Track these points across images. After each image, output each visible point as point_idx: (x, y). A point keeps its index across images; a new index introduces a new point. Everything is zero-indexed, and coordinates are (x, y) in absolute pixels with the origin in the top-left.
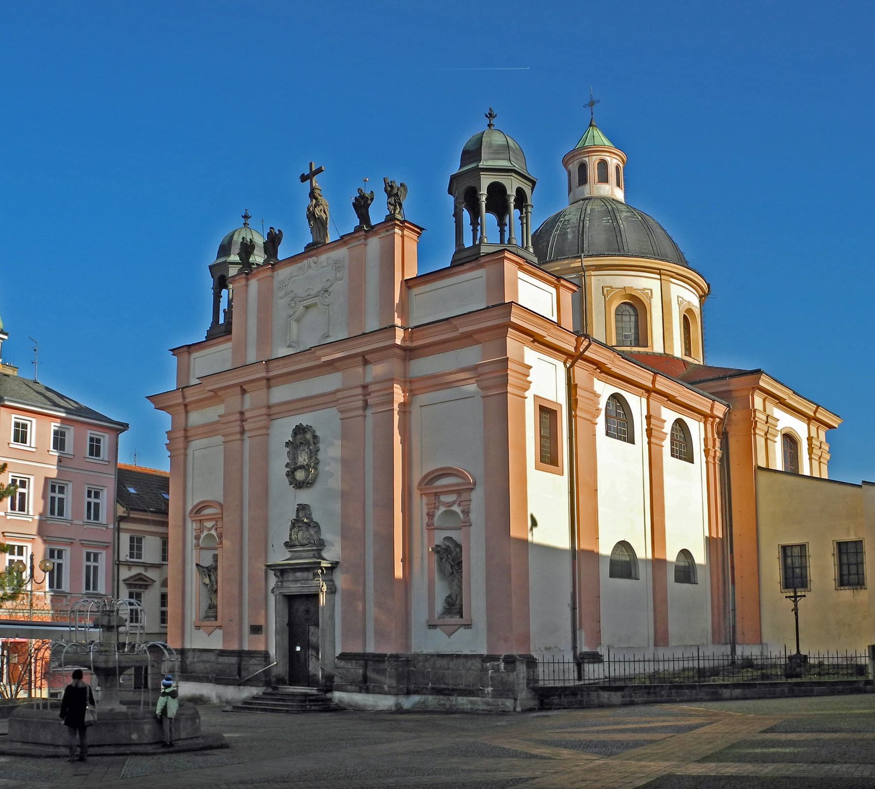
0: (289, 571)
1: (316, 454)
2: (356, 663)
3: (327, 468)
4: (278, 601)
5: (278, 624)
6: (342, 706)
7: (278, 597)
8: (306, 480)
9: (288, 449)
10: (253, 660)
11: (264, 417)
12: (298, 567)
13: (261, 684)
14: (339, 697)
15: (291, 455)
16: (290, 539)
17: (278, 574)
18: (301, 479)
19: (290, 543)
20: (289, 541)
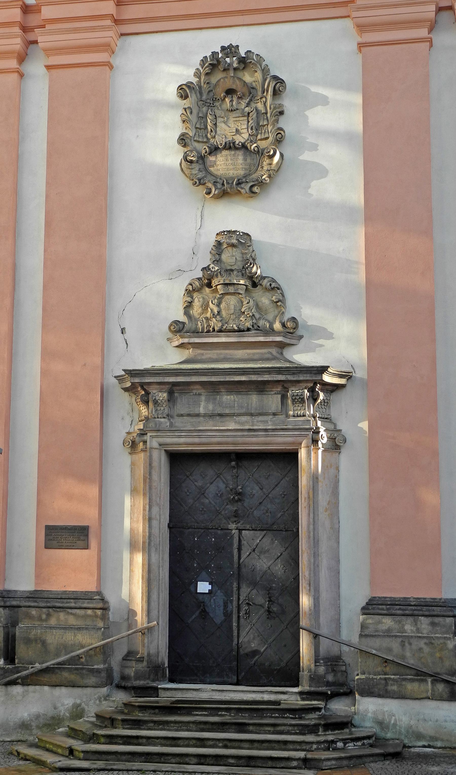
0: (197, 389)
1: (277, 121)
2: (433, 624)
3: (306, 156)
4: (155, 464)
5: (155, 523)
6: (389, 735)
7: (155, 454)
8: (245, 176)
9: (186, 103)
10: (62, 615)
11: (108, 22)
12: (243, 378)
13: (92, 680)
14: (374, 713)
15: (194, 118)
16: (187, 313)
17: (163, 396)
18: (231, 173)
19: (187, 327)
20: (182, 318)
